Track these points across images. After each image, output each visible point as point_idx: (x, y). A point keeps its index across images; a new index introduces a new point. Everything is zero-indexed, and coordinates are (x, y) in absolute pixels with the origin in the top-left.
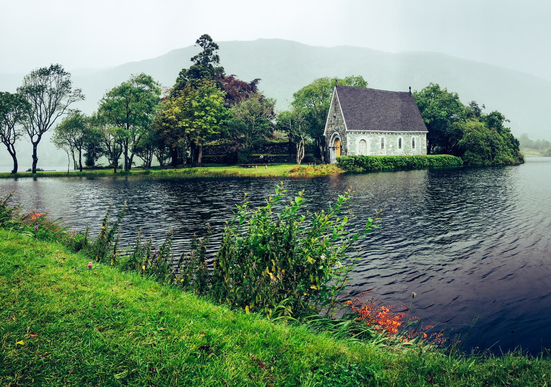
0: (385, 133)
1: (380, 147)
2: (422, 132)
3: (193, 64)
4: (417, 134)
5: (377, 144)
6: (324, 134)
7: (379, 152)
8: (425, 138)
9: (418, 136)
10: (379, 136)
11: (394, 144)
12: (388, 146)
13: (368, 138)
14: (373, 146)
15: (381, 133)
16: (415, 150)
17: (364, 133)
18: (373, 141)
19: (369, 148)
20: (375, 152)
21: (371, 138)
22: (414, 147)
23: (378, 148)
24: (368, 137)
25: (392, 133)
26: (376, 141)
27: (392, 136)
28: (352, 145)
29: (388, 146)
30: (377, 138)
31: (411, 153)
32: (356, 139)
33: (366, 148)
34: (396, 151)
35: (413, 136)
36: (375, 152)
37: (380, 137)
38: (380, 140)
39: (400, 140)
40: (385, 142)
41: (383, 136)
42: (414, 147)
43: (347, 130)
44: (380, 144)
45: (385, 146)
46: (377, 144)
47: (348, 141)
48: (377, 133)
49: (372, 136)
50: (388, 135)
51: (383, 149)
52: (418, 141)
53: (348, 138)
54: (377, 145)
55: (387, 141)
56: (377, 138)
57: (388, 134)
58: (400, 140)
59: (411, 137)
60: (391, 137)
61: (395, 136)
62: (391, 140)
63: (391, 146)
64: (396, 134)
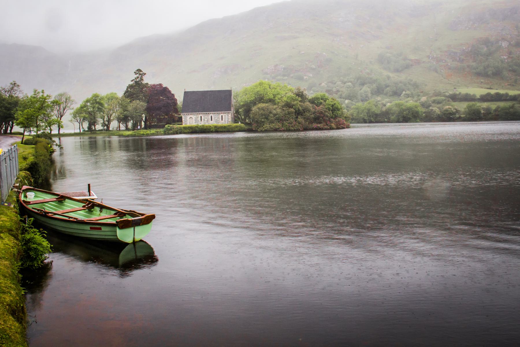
0: (202, 114)
3: (132, 83)
4: (224, 113)
12: (204, 120)
13: (194, 117)
14: (196, 120)
15: (199, 114)
16: (223, 121)
17: (191, 114)
19: (194, 121)
21: (195, 117)
22: (212, 120)
23: (198, 121)
25: (206, 113)
34: (209, 122)
35: (221, 115)
37: (200, 116)
38: (200, 117)
39: (211, 117)
40: (203, 118)
41: (201, 115)
42: (212, 120)
44: (199, 119)
45: (202, 120)
48: (198, 114)
57: (204, 114)
58: (211, 117)
62: (206, 116)
63: (206, 120)
64: (208, 114)
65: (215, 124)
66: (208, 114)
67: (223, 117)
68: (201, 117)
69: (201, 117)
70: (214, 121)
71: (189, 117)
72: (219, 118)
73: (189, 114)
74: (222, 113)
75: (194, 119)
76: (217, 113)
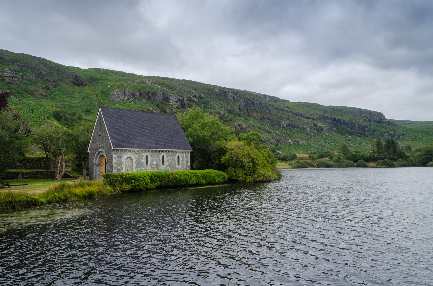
0: (149, 151)
1: (145, 164)
2: (186, 150)
4: (182, 152)
5: (142, 161)
6: (88, 151)
7: (143, 168)
8: (189, 156)
9: (183, 154)
10: (144, 154)
11: (158, 161)
12: (152, 163)
13: (134, 157)
14: (137, 163)
15: (145, 151)
16: (180, 166)
17: (130, 151)
18: (138, 158)
19: (134, 165)
20: (139, 169)
21: (136, 156)
23: (143, 165)
24: (134, 155)
25: (156, 151)
26: (141, 158)
27: (156, 154)
28: (118, 162)
29: (152, 163)
30: (142, 156)
31: (176, 169)
32: (122, 157)
33: (132, 165)
34: (159, 167)
35: (178, 154)
36: (139, 169)
37: (145, 155)
38: (145, 157)
39: (163, 157)
41: (147, 154)
43: (112, 148)
44: (144, 161)
45: (149, 163)
46: (142, 161)
47: (114, 158)
48: (142, 151)
49: (136, 154)
50: (152, 153)
51: (147, 166)
52: (183, 159)
53: (114, 156)
54: (142, 162)
55: (151, 159)
56: (142, 156)
57: (152, 151)
58: (163, 157)
59: (176, 155)
60: (155, 155)
61: (159, 153)
63: (155, 163)
64: (159, 152)
65: (170, 171)
66: (159, 152)
67: (181, 159)
68: (147, 157)
69: (147, 157)
70: (167, 166)
71: (125, 156)
72: (174, 160)
73: (126, 151)
74: (179, 152)
75: (134, 160)
76: (172, 152)
